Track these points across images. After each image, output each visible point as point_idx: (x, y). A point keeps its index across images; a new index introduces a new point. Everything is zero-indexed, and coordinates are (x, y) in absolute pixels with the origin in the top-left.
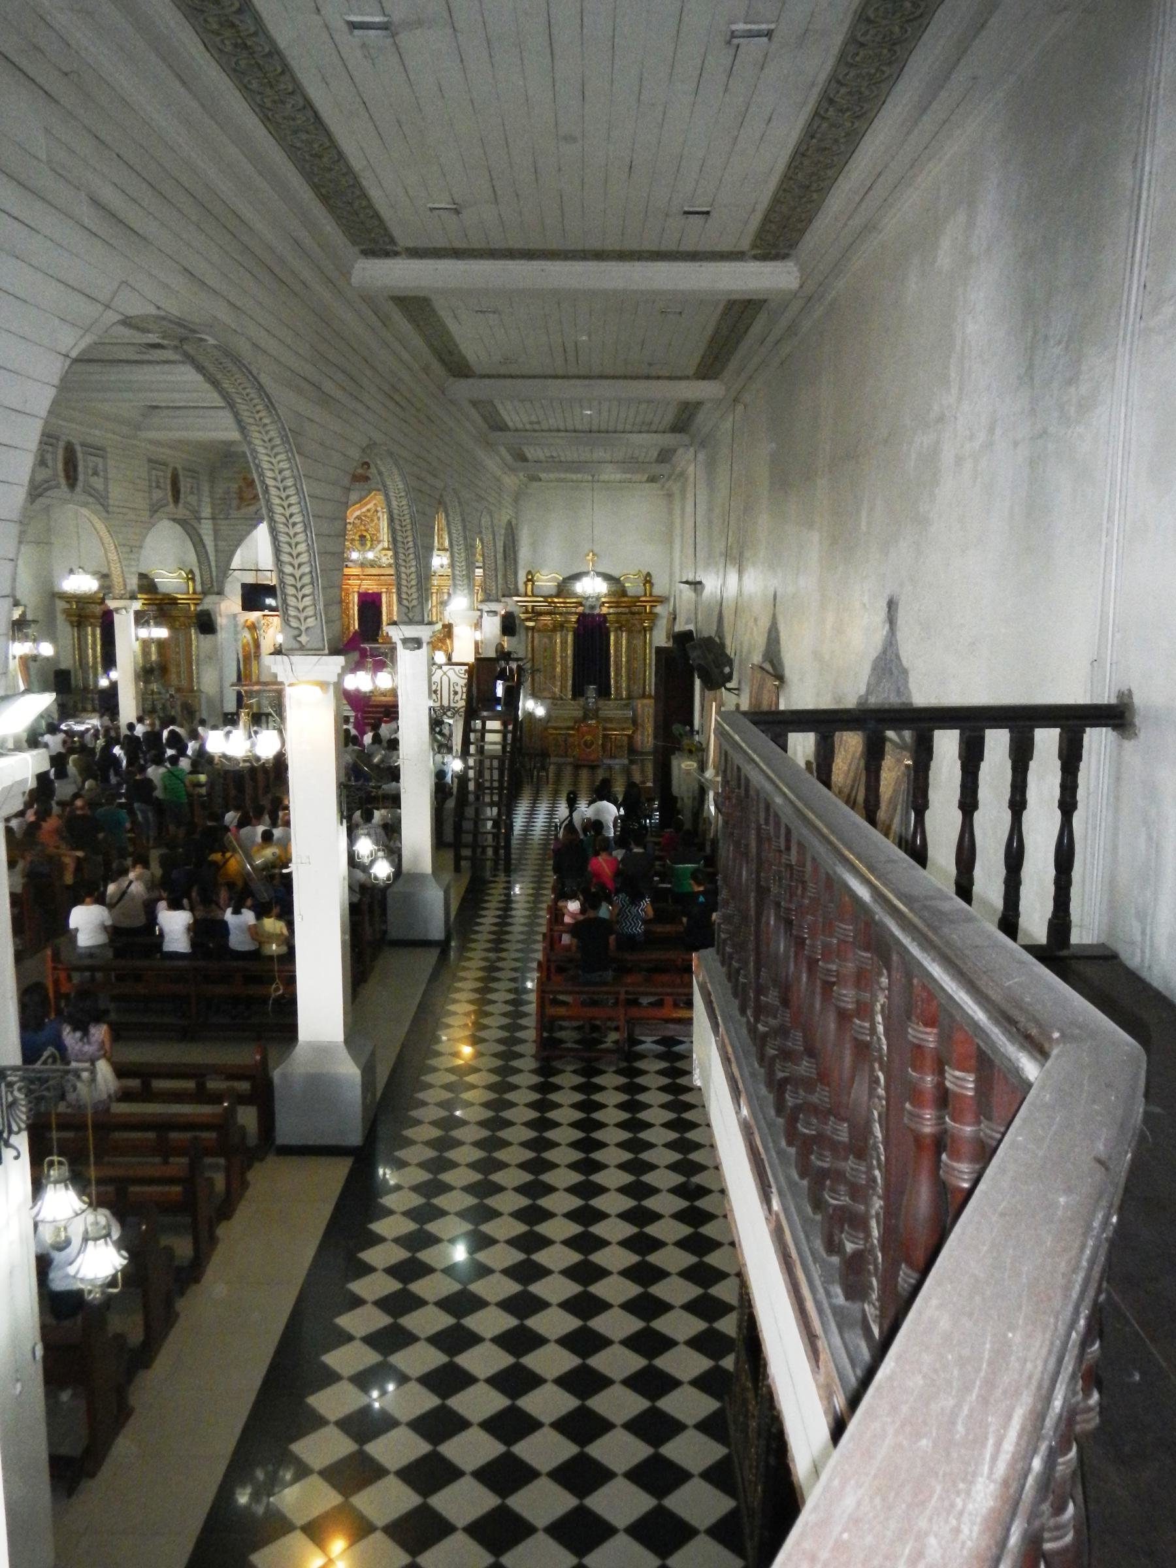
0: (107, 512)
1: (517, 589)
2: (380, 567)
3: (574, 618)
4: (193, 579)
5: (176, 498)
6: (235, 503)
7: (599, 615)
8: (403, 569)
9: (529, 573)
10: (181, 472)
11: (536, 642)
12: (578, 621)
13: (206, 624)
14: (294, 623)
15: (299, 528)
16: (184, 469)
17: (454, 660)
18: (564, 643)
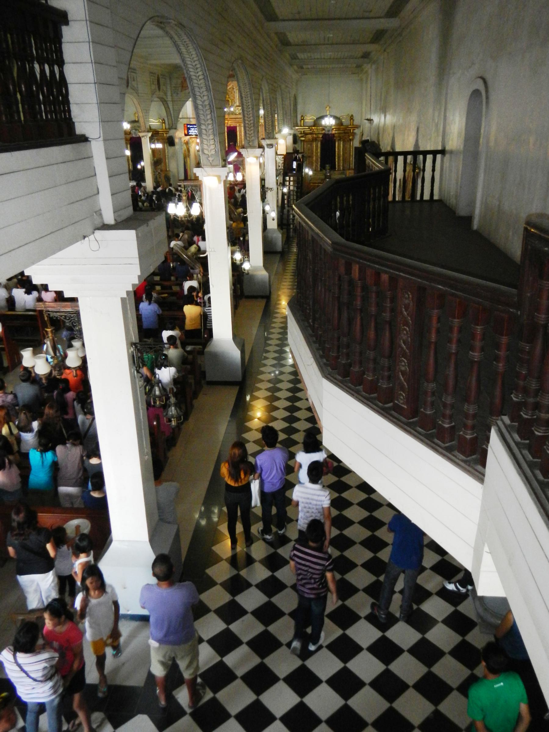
0: (138, 96)
1: (297, 123)
2: (236, 114)
3: (321, 136)
4: (165, 123)
5: (159, 89)
6: (180, 89)
7: (331, 134)
8: (267, 119)
9: (302, 116)
10: (160, 76)
11: (305, 146)
12: (322, 137)
13: (171, 142)
14: (248, 139)
15: (250, 109)
16: (161, 75)
17: (278, 153)
18: (317, 146)
